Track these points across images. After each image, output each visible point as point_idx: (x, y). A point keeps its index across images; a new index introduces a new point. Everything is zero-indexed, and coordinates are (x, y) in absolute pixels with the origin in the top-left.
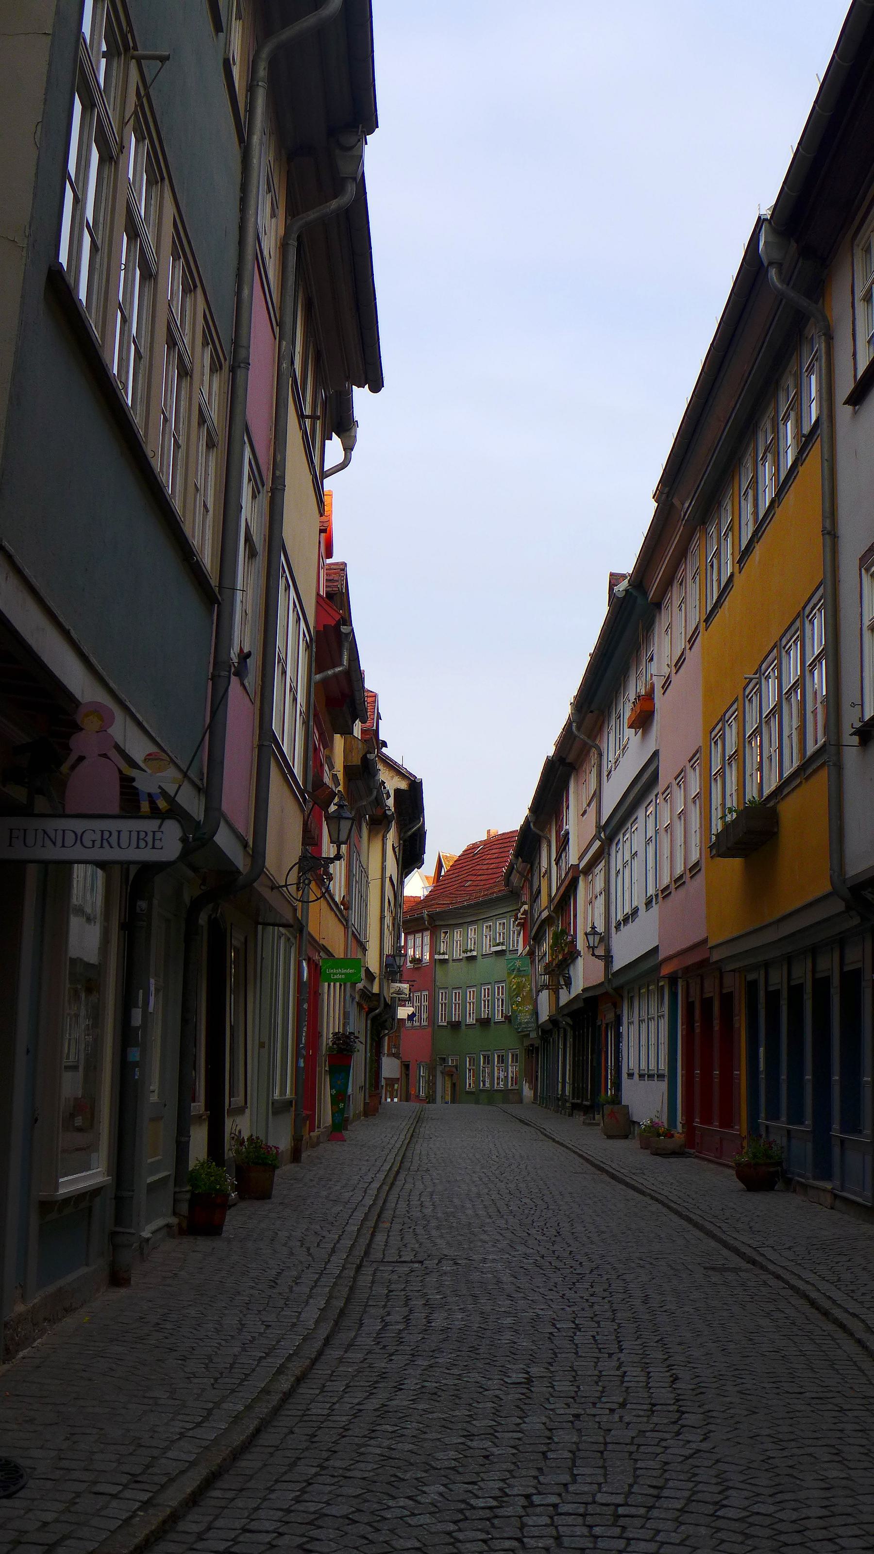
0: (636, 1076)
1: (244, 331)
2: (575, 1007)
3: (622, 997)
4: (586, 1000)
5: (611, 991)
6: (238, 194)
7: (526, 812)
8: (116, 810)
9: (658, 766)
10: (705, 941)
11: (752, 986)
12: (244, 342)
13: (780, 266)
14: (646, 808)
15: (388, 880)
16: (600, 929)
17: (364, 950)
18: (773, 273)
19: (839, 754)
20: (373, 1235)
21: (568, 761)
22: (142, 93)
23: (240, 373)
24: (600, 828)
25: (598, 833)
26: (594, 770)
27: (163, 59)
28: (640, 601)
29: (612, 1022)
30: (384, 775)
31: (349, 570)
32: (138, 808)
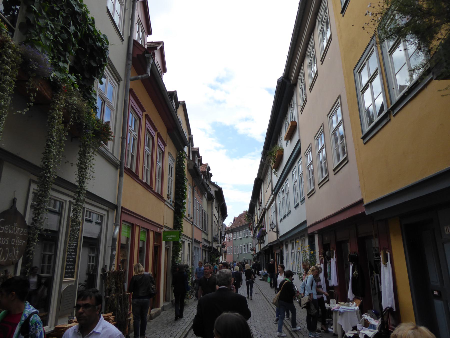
2: (266, 248)
7: (250, 199)
9: (300, 145)
14: (292, 172)
16: (275, 222)
17: (207, 234)
21: (261, 179)
24: (273, 191)
25: (272, 192)
26: (270, 173)
28: (288, 83)
29: (278, 253)
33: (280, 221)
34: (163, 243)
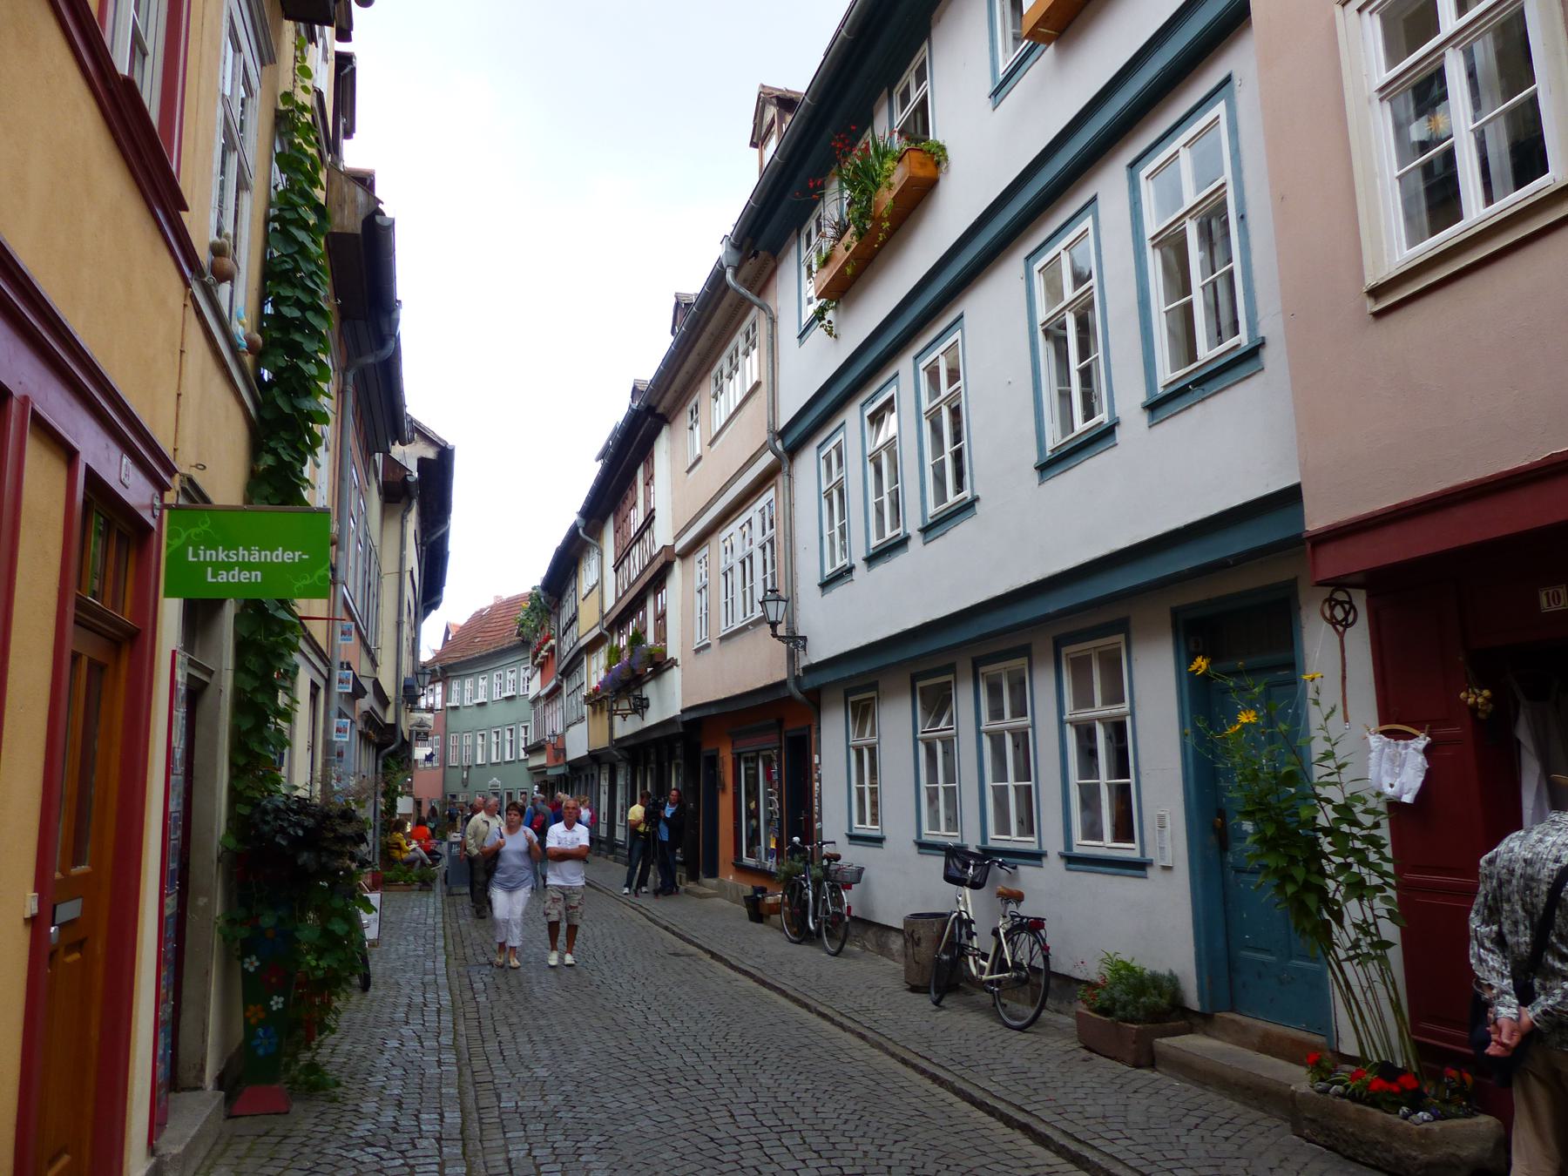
2: (655, 735)
4: (685, 724)
5: (798, 695)
21: (660, 410)
33: (826, 584)
34: (171, 612)
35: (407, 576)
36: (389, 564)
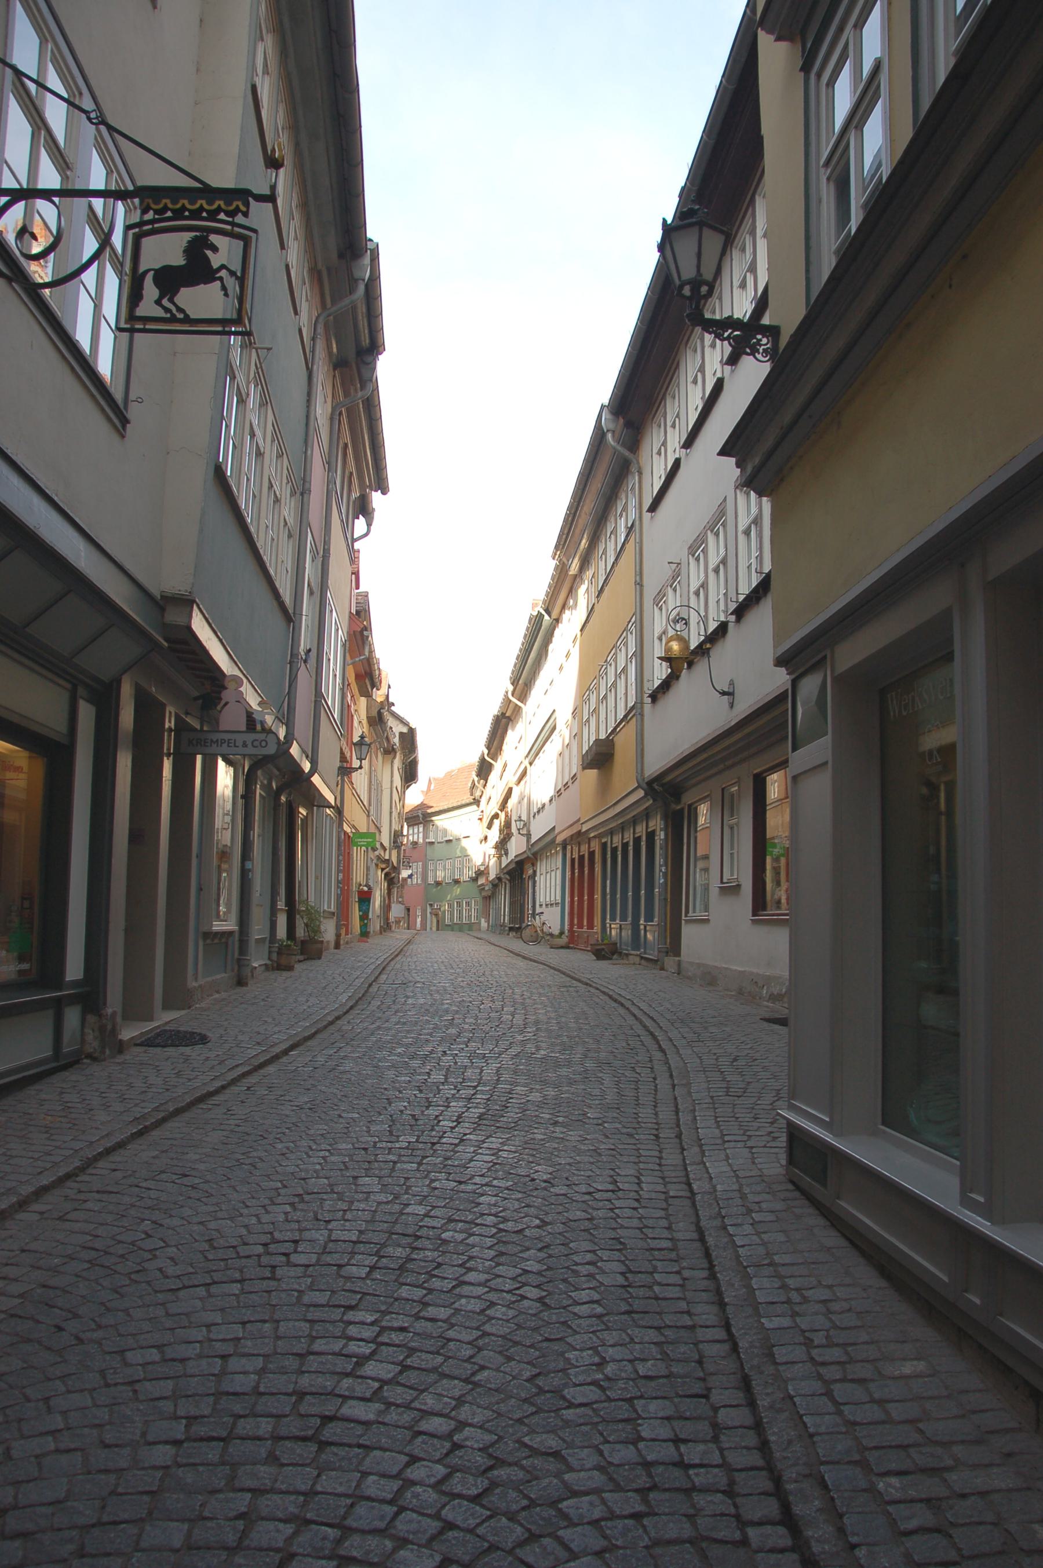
0: (544, 906)
1: (308, 473)
3: (537, 859)
4: (517, 863)
5: (530, 855)
6: (305, 398)
8: (244, 729)
10: (579, 820)
11: (604, 846)
12: (308, 479)
13: (613, 432)
15: (394, 789)
16: (524, 817)
18: (609, 436)
19: (642, 708)
20: (380, 974)
21: (507, 715)
22: (259, 366)
23: (306, 496)
27: (269, 349)
30: (391, 722)
31: (369, 595)
32: (255, 729)
33: (534, 817)
35: (394, 789)
36: (386, 785)
